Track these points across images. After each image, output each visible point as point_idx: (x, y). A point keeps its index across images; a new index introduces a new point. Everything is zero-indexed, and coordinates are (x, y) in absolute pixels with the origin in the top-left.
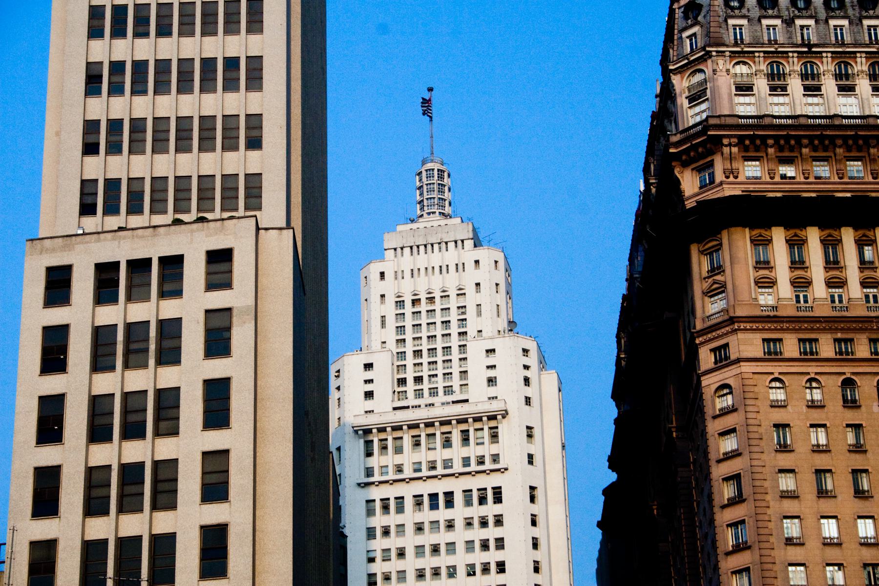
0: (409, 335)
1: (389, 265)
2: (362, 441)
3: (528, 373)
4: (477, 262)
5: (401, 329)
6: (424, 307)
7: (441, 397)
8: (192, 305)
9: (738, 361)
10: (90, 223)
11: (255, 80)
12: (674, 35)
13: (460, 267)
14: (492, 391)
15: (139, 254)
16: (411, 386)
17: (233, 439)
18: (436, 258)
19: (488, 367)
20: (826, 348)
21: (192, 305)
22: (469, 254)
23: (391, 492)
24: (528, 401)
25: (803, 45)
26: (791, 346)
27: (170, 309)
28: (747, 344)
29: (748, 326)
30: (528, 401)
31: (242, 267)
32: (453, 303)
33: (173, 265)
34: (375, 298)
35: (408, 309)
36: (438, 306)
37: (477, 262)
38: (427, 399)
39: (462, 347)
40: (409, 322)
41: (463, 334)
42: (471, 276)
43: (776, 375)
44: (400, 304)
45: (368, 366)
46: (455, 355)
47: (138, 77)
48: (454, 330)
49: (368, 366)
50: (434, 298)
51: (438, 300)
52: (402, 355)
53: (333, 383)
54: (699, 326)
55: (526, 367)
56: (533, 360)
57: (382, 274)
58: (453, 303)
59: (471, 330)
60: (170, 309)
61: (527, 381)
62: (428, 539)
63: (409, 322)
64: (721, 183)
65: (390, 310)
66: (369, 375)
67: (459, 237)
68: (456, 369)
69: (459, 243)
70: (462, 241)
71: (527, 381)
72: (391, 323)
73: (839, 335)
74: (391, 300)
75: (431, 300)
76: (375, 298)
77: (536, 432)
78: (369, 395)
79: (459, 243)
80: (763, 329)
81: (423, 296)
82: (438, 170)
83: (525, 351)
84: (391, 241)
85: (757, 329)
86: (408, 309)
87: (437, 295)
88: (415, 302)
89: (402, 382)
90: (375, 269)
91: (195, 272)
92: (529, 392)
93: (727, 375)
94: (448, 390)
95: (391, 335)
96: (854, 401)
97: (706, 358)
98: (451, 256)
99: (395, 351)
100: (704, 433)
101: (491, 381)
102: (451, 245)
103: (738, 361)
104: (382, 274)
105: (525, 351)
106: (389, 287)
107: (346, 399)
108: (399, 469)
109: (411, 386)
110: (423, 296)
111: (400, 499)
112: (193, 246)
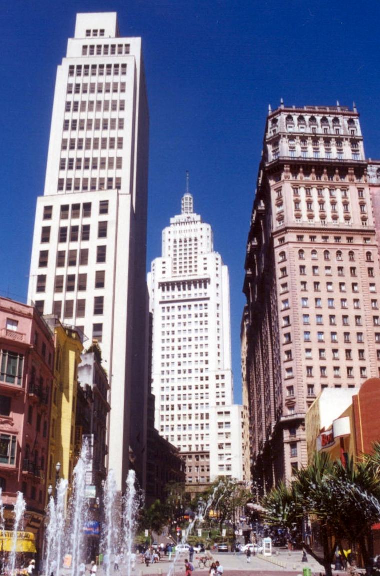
0: (178, 253)
1: (172, 228)
2: (161, 288)
4: (202, 229)
5: (175, 251)
6: (183, 243)
7: (188, 273)
8: (94, 220)
9: (288, 243)
10: (61, 192)
11: (120, 146)
12: (269, 111)
14: (205, 272)
15: (76, 202)
16: (178, 270)
17: (107, 267)
20: (319, 239)
21: (94, 220)
22: (200, 225)
23: (171, 305)
24: (217, 275)
25: (314, 134)
26: (307, 238)
27: (86, 221)
28: (291, 237)
29: (292, 230)
30: (217, 275)
31: (112, 208)
33: (88, 207)
34: (167, 241)
35: (178, 244)
36: (188, 243)
37: (202, 229)
38: (184, 273)
39: (196, 257)
43: (301, 248)
44: (175, 242)
45: (164, 263)
46: (193, 260)
47: (79, 144)
48: (193, 251)
49: (164, 263)
51: (188, 241)
52: (175, 259)
53: (152, 268)
54: (275, 230)
55: (217, 264)
56: (220, 261)
57: (170, 232)
58: (193, 242)
59: (199, 251)
60: (86, 221)
61: (217, 269)
62: (183, 320)
63: (178, 248)
64: (284, 181)
65: (172, 244)
66: (164, 265)
68: (193, 264)
72: (172, 248)
73: (324, 235)
74: (172, 241)
75: (186, 241)
76: (167, 241)
78: (164, 272)
80: (297, 232)
81: (183, 240)
83: (217, 259)
84: (173, 220)
85: (295, 232)
86: (178, 244)
88: (181, 241)
89: (175, 268)
90: (166, 230)
91: (96, 208)
93: (284, 248)
95: (172, 253)
96: (328, 258)
97: (277, 242)
98: (193, 226)
99: (173, 257)
100: (276, 285)
101: (206, 269)
103: (288, 243)
104: (170, 232)
105: (217, 259)
106: (173, 238)
107: (156, 274)
108: (173, 297)
109: (178, 270)
110: (183, 240)
111: (173, 307)
112: (94, 198)
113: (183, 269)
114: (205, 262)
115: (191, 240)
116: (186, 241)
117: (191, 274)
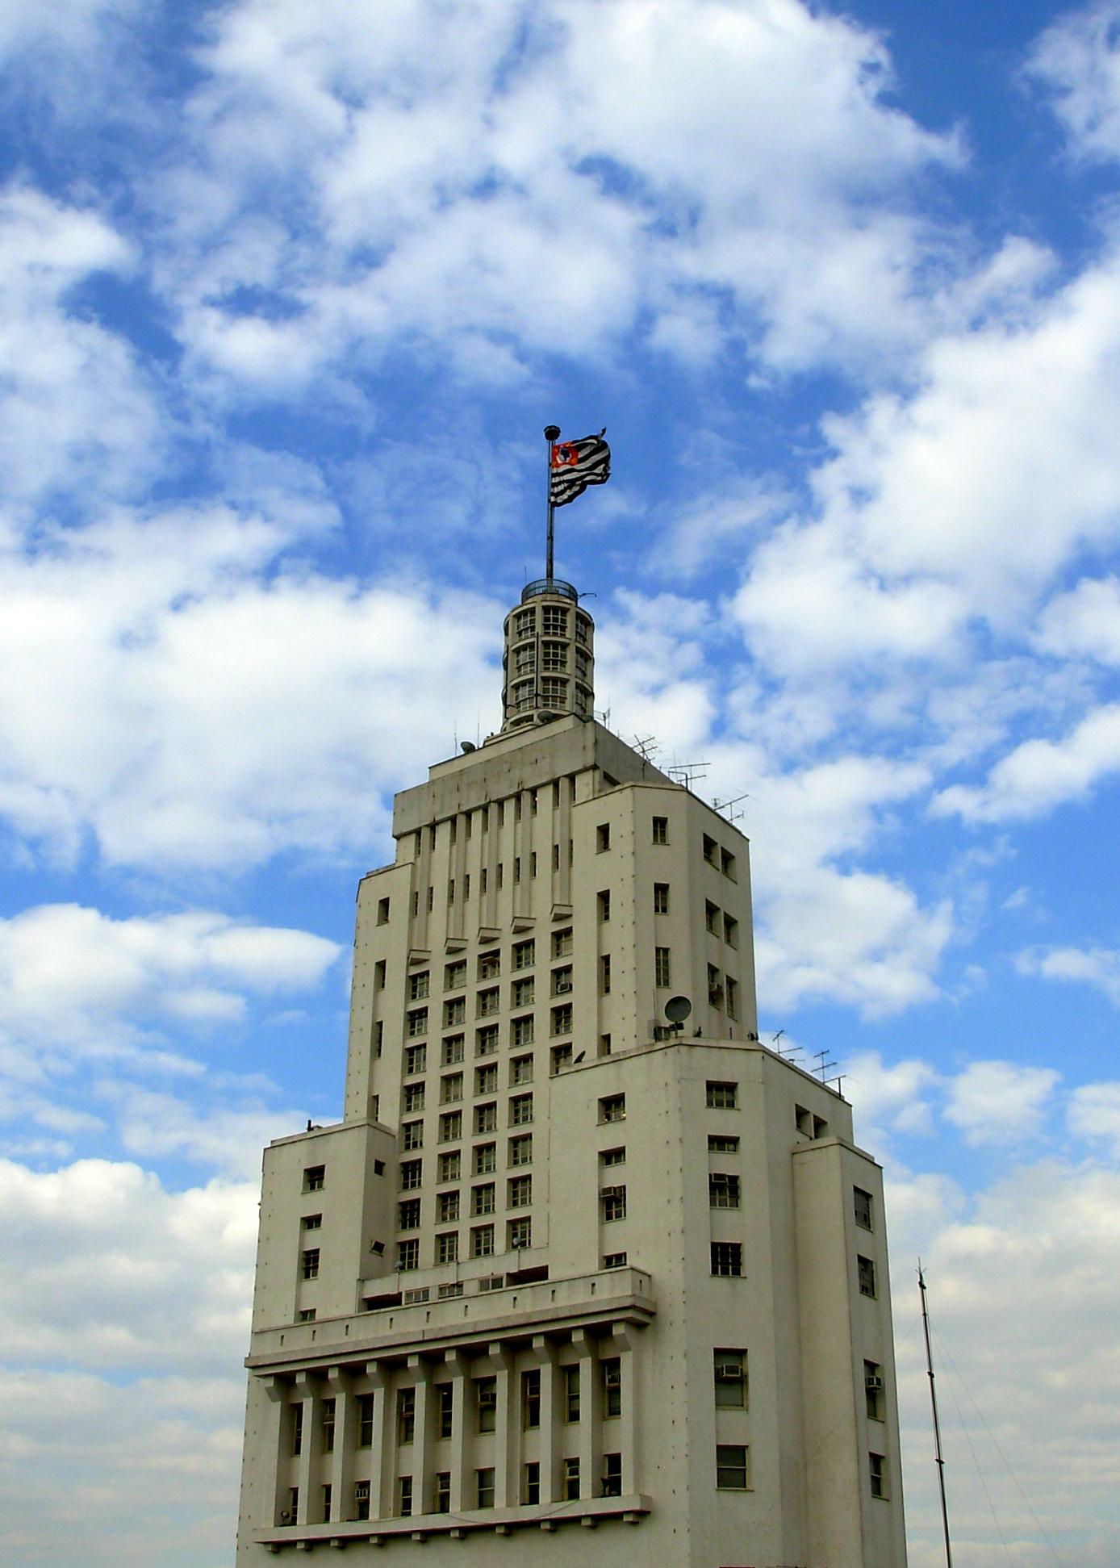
0: (432, 1073)
2: (276, 1408)
3: (726, 1164)
4: (604, 831)
5: (413, 1056)
13: (562, 855)
16: (428, 1229)
18: (509, 839)
19: (611, 1157)
24: (727, 1259)
30: (727, 1259)
32: (542, 966)
40: (434, 1033)
41: (561, 1053)
42: (592, 872)
44: (416, 984)
48: (542, 1042)
50: (497, 953)
52: (410, 1134)
55: (721, 1143)
58: (542, 966)
59: (582, 1036)
61: (725, 1189)
65: (394, 1004)
67: (563, 769)
69: (564, 784)
70: (571, 778)
71: (725, 1189)
74: (397, 977)
75: (490, 961)
77: (757, 1369)
78: (310, 1262)
79: (564, 784)
82: (546, 610)
86: (435, 998)
87: (505, 945)
89: (409, 1213)
92: (731, 1226)
94: (519, 1232)
95: (391, 1080)
101: (613, 1202)
102: (545, 796)
104: (385, 903)
113: (465, 1222)
114: (611, 1137)
115: (523, 951)
116: (490, 961)
117: (488, 1267)
